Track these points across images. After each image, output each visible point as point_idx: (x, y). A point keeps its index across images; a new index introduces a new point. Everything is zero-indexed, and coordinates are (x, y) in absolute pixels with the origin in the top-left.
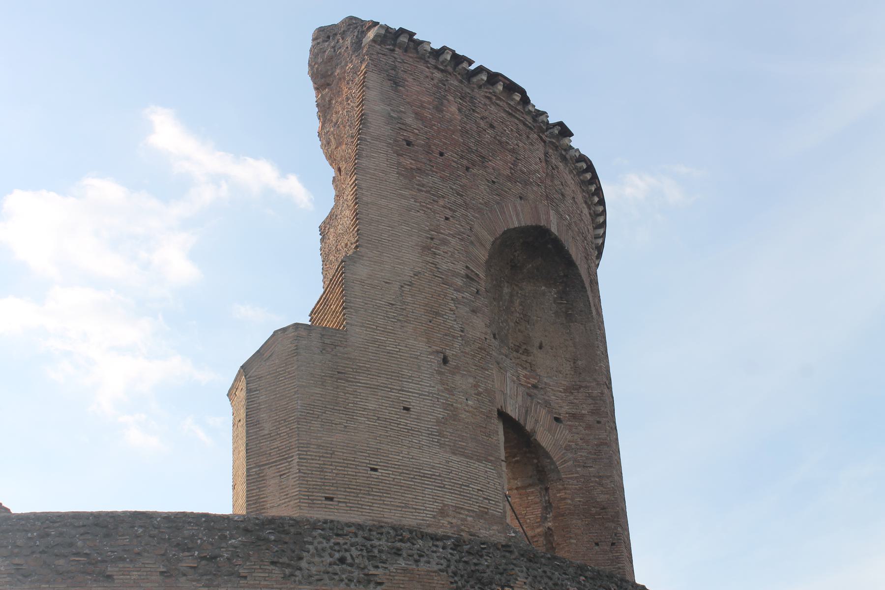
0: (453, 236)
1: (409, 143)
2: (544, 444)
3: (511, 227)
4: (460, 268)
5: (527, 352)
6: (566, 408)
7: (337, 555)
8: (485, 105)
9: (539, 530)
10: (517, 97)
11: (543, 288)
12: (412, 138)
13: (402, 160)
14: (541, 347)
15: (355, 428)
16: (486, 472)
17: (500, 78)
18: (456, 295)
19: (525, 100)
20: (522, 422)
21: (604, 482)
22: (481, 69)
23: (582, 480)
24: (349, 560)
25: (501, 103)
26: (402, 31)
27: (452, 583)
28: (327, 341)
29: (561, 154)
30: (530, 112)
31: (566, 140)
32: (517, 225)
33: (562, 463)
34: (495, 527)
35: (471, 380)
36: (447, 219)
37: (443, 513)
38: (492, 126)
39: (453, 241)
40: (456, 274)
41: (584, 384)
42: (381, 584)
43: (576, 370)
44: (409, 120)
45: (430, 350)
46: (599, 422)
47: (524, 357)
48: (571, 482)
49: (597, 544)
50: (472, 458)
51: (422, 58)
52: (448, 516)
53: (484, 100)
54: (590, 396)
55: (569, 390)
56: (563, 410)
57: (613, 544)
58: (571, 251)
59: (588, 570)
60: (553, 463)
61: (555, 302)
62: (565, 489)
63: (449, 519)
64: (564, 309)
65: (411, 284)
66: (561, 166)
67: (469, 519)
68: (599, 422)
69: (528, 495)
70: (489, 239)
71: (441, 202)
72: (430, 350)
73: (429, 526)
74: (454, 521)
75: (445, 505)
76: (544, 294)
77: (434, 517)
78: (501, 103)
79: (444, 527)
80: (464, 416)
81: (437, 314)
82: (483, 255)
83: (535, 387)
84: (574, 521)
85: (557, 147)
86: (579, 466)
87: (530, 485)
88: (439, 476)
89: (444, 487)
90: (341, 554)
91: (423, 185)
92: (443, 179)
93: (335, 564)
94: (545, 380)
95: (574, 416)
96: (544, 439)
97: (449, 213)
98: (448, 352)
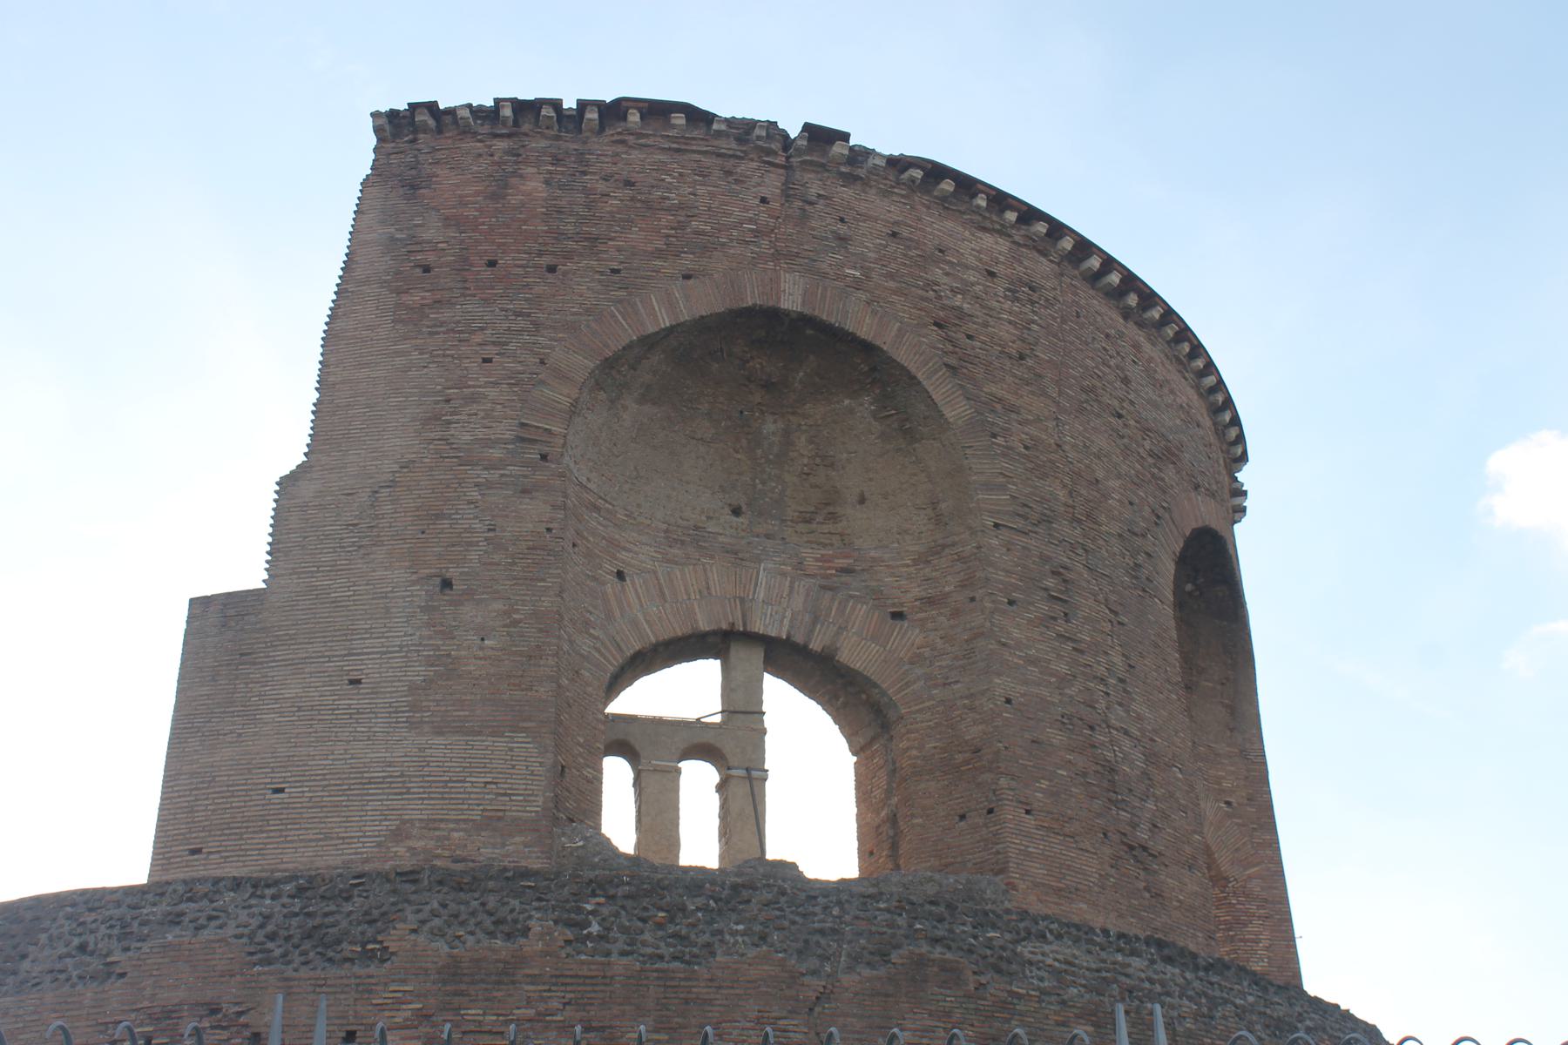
0: (495, 384)
1: (427, 269)
2: (857, 666)
3: (651, 329)
4: (505, 430)
5: (833, 517)
6: (916, 591)
7: (76, 941)
8: (617, 154)
9: (883, 814)
10: (679, 119)
11: (847, 402)
12: (431, 258)
13: (405, 298)
14: (862, 500)
15: (255, 734)
16: (511, 749)
17: (624, 104)
18: (485, 474)
20: (799, 638)
21: (977, 703)
22: (583, 105)
23: (941, 709)
24: (91, 947)
25: (650, 142)
26: (413, 107)
27: (251, 954)
28: (232, 612)
29: (842, 175)
30: (719, 133)
31: (838, 149)
32: (666, 322)
33: (901, 689)
34: (518, 839)
35: (498, 606)
36: (486, 361)
37: (398, 835)
38: (629, 184)
39: (492, 393)
40: (489, 443)
41: (949, 541)
42: (122, 975)
43: (939, 520)
44: (432, 231)
45: (414, 577)
46: (973, 599)
47: (826, 528)
48: (919, 717)
49: (963, 817)
50: (480, 733)
51: (466, 132)
52: (408, 837)
53: (610, 150)
54: (961, 559)
55: (922, 560)
56: (909, 595)
57: (990, 811)
58: (849, 326)
59: (623, 883)
60: (883, 693)
61: (874, 415)
62: (908, 732)
63: (411, 843)
64: (895, 425)
65: (392, 484)
66: (847, 193)
67: (456, 835)
68: (973, 599)
69: (873, 757)
70: (582, 365)
71: (478, 338)
72: (414, 577)
73: (366, 861)
74: (419, 844)
75: (404, 822)
76: (851, 411)
77: (379, 845)
78: (650, 142)
79: (402, 856)
80: (472, 668)
81: (440, 516)
82: (561, 396)
83: (847, 571)
84: (923, 785)
85: (823, 165)
86: (936, 686)
87: (873, 740)
88: (402, 776)
89: (408, 793)
90: (84, 938)
91: (442, 324)
92: (486, 301)
93: (69, 955)
94: (873, 553)
95: (930, 601)
96: (856, 654)
97: (490, 351)
98: (452, 573)
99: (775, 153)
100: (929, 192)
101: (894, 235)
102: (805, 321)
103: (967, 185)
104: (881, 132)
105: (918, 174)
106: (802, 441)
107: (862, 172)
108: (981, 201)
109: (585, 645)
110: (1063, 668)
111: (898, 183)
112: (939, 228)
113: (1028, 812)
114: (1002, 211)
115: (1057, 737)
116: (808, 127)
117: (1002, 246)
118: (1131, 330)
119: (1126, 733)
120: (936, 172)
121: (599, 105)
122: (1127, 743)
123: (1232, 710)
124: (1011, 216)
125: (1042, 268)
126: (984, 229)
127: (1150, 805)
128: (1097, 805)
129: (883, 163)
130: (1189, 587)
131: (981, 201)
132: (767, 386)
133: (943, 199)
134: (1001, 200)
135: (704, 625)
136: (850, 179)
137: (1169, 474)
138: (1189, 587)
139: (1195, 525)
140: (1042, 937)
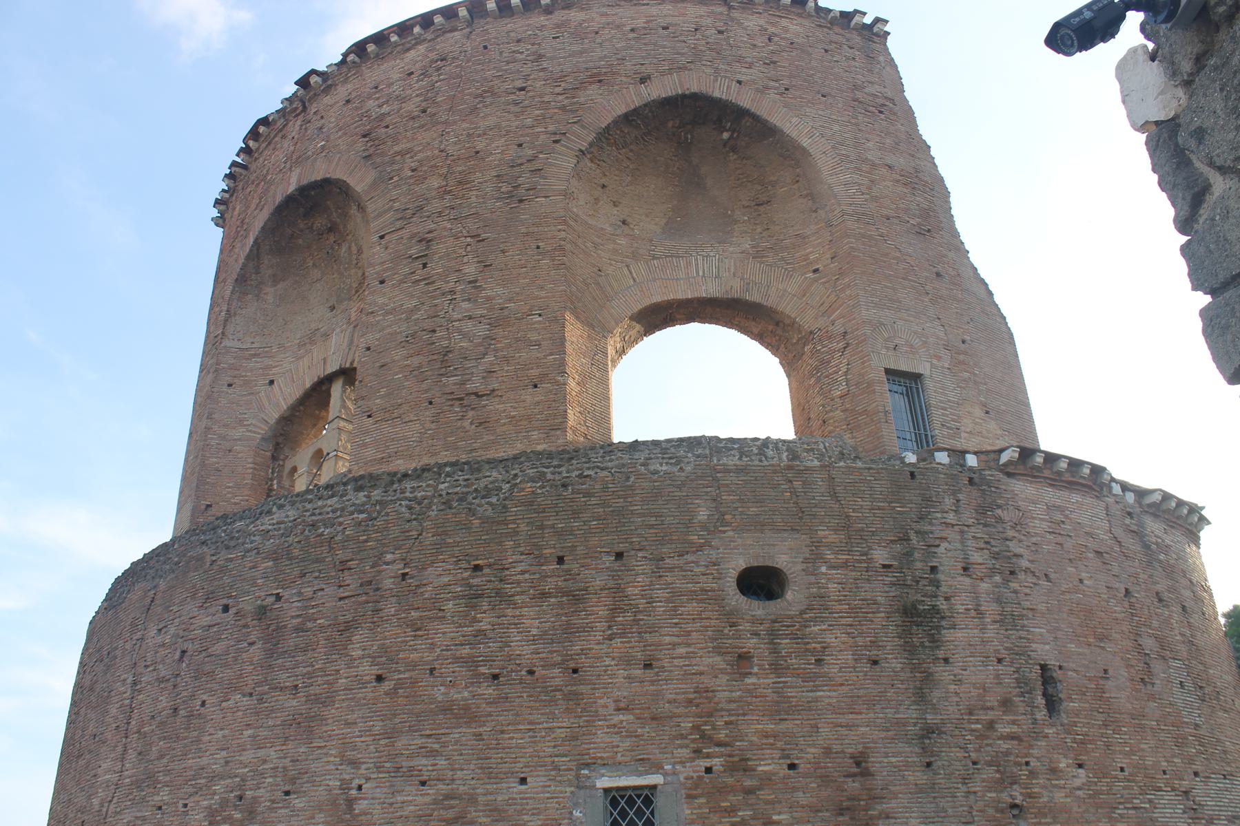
10: (262, 129)
19: (264, 121)
22: (238, 155)
31: (314, 79)
99: (296, 109)
100: (369, 58)
101: (348, 101)
102: (303, 190)
103: (379, 38)
104: (328, 54)
105: (351, 57)
106: (354, 249)
107: (329, 82)
108: (394, 38)
109: (238, 433)
110: (414, 302)
111: (349, 71)
112: (373, 74)
113: (369, 416)
114: (433, 23)
115: (398, 354)
116: (296, 83)
117: (422, 48)
118: (559, 16)
119: (470, 318)
120: (359, 48)
121: (242, 150)
122: (468, 326)
123: (811, 196)
124: (417, 30)
125: (452, 42)
126: (409, 50)
127: (489, 358)
128: (424, 386)
129: (335, 68)
130: (726, 135)
131: (394, 38)
132: (332, 229)
133: (377, 56)
134: (403, 28)
135: (308, 385)
136: (327, 90)
137: (593, 91)
138: (726, 135)
139: (621, 110)
140: (269, 512)
